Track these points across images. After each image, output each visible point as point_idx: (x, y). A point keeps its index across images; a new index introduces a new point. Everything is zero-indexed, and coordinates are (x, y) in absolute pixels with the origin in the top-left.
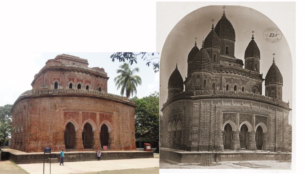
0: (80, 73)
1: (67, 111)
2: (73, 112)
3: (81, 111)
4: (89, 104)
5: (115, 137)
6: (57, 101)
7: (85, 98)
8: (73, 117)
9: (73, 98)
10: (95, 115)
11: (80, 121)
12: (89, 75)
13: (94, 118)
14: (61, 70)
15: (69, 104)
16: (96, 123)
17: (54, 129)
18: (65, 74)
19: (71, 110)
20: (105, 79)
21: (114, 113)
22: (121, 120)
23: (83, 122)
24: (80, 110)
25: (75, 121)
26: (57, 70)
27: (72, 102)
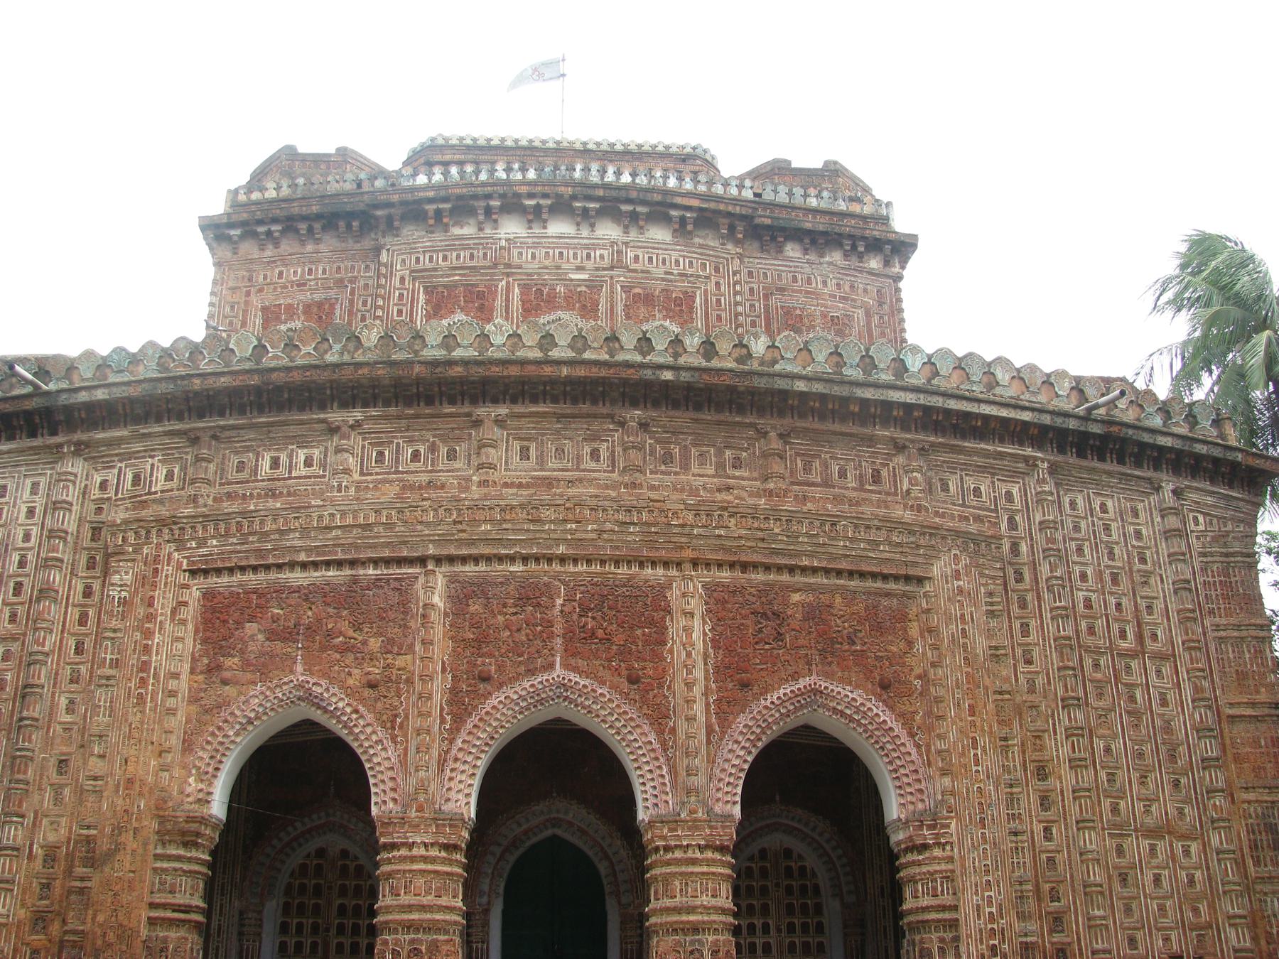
0: (559, 227)
1: (251, 579)
2: (323, 592)
3: (445, 568)
4: (549, 483)
5: (969, 900)
6: (137, 479)
7: (481, 411)
8: (324, 649)
9: (333, 430)
10: (652, 612)
11: (425, 697)
12: (660, 234)
13: (624, 653)
14: (342, 224)
15: (273, 494)
16: (660, 717)
17: (58, 800)
18: (384, 256)
19: (304, 566)
20: (874, 263)
21: (936, 570)
22: (1047, 658)
23: (460, 707)
24: (422, 561)
25: (350, 692)
26: (303, 227)
27: (315, 469)
